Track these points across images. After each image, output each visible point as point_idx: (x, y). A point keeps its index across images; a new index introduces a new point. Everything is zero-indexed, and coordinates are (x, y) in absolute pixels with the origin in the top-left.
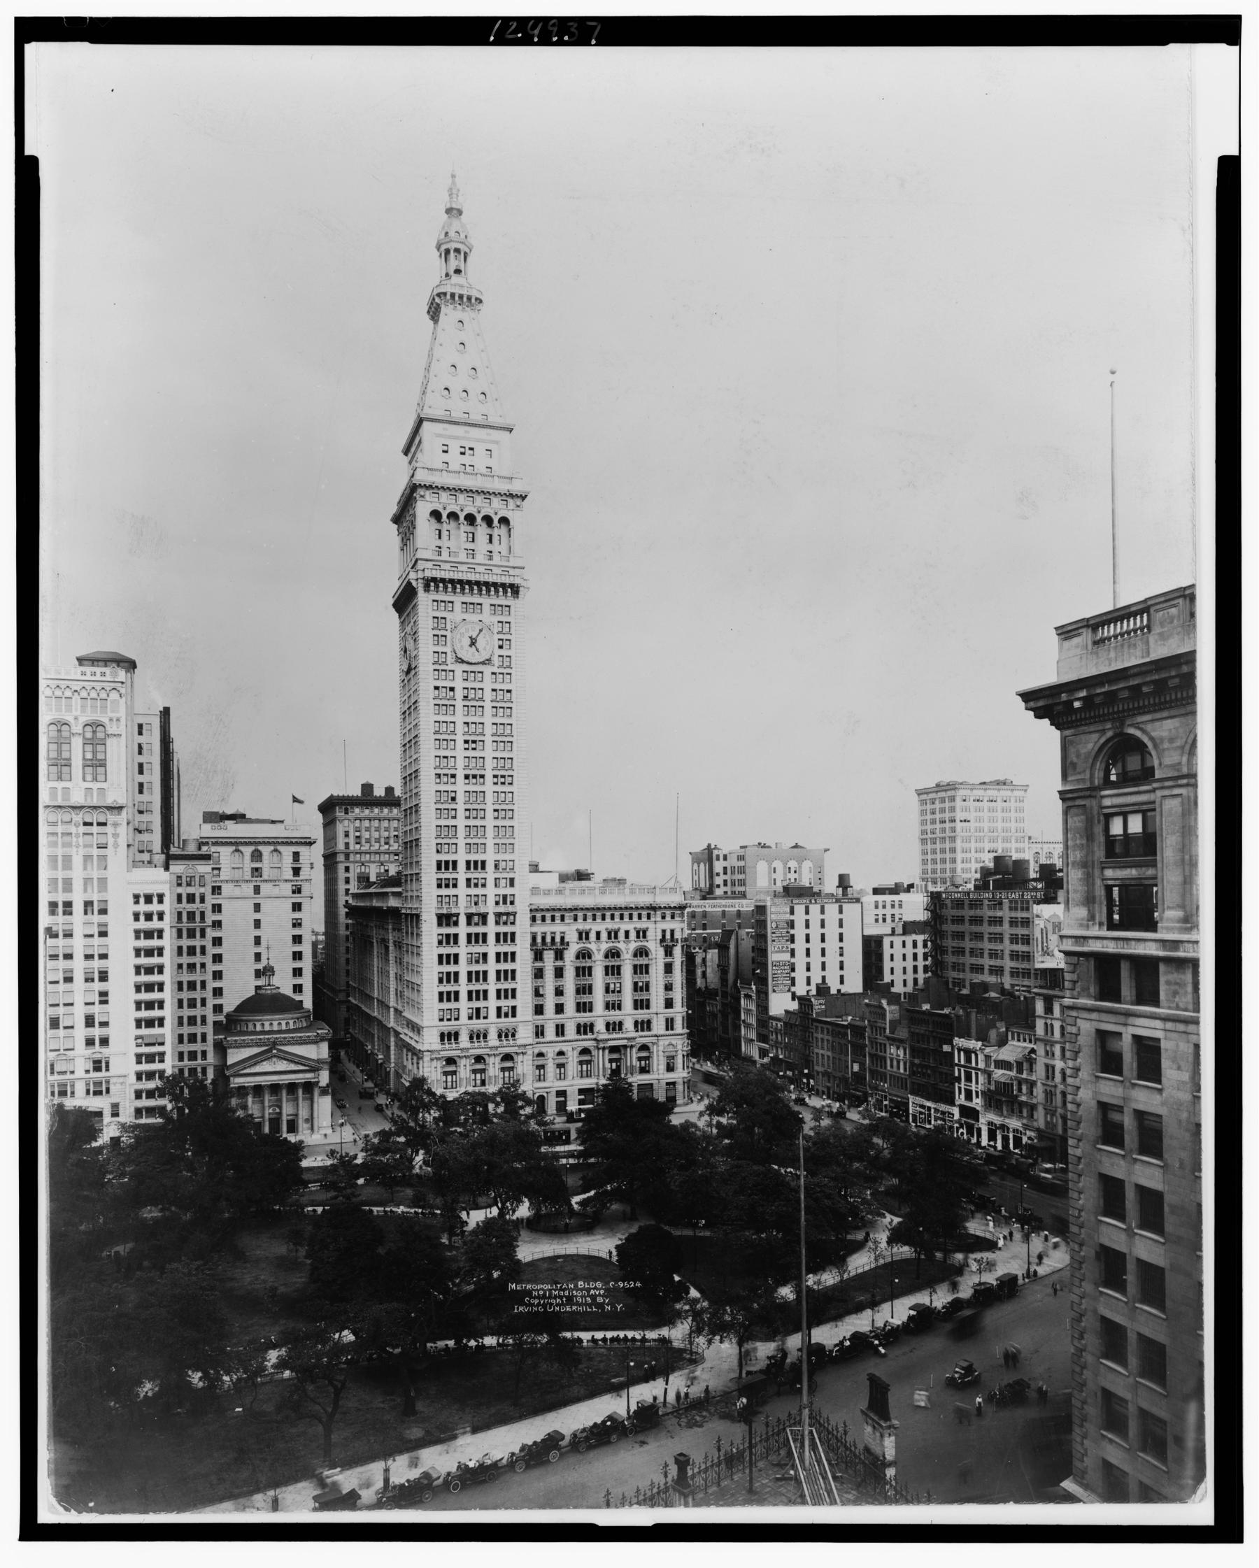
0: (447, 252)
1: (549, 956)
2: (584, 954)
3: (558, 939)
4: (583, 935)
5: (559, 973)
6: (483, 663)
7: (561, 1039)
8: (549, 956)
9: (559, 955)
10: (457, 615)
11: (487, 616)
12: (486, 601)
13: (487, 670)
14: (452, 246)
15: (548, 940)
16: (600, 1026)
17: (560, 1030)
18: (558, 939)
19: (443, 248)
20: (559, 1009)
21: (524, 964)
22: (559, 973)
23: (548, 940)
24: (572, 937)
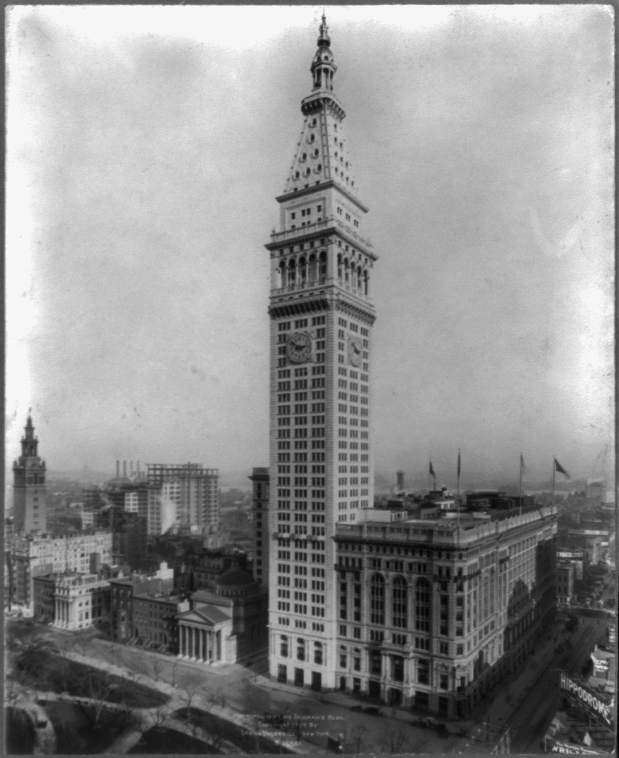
0: (319, 72)
1: (349, 576)
2: (377, 578)
3: (357, 564)
4: (376, 563)
5: (358, 589)
6: (306, 362)
7: (357, 639)
8: (349, 576)
9: (357, 575)
10: (293, 331)
11: (311, 329)
12: (309, 317)
13: (309, 366)
14: (324, 66)
15: (350, 564)
16: (387, 635)
17: (357, 633)
18: (357, 564)
19: (317, 68)
20: (358, 616)
21: (332, 580)
22: (358, 589)
23: (350, 564)
24: (366, 563)
